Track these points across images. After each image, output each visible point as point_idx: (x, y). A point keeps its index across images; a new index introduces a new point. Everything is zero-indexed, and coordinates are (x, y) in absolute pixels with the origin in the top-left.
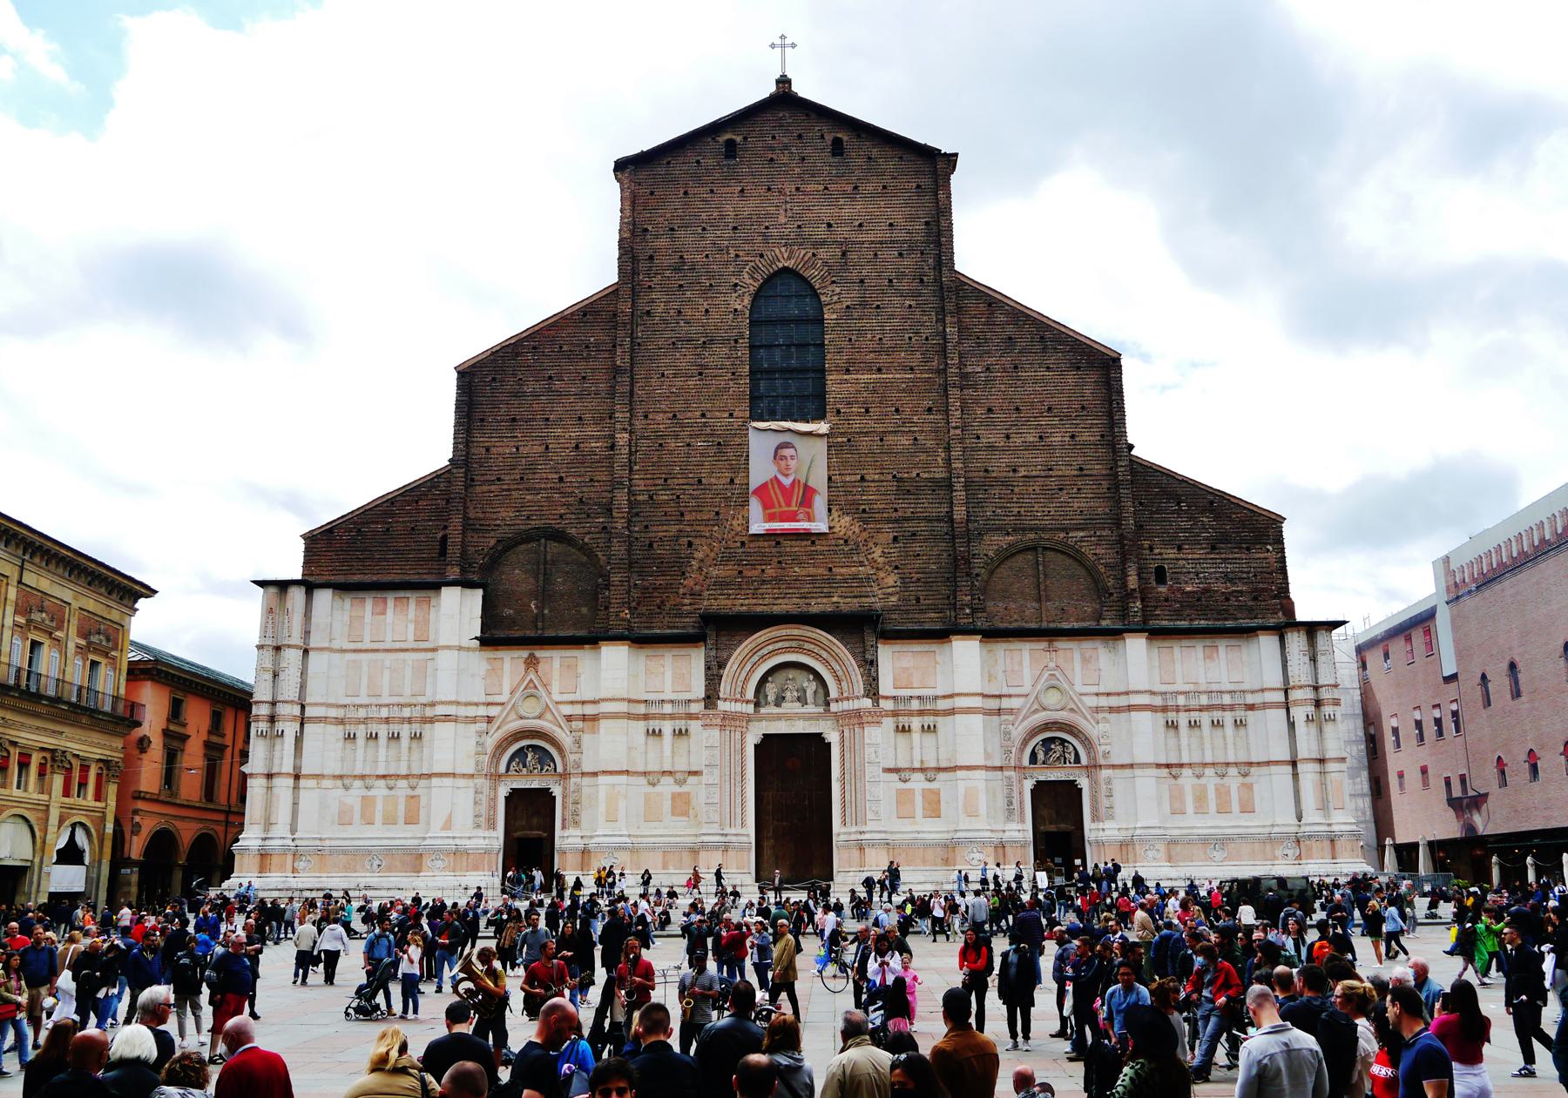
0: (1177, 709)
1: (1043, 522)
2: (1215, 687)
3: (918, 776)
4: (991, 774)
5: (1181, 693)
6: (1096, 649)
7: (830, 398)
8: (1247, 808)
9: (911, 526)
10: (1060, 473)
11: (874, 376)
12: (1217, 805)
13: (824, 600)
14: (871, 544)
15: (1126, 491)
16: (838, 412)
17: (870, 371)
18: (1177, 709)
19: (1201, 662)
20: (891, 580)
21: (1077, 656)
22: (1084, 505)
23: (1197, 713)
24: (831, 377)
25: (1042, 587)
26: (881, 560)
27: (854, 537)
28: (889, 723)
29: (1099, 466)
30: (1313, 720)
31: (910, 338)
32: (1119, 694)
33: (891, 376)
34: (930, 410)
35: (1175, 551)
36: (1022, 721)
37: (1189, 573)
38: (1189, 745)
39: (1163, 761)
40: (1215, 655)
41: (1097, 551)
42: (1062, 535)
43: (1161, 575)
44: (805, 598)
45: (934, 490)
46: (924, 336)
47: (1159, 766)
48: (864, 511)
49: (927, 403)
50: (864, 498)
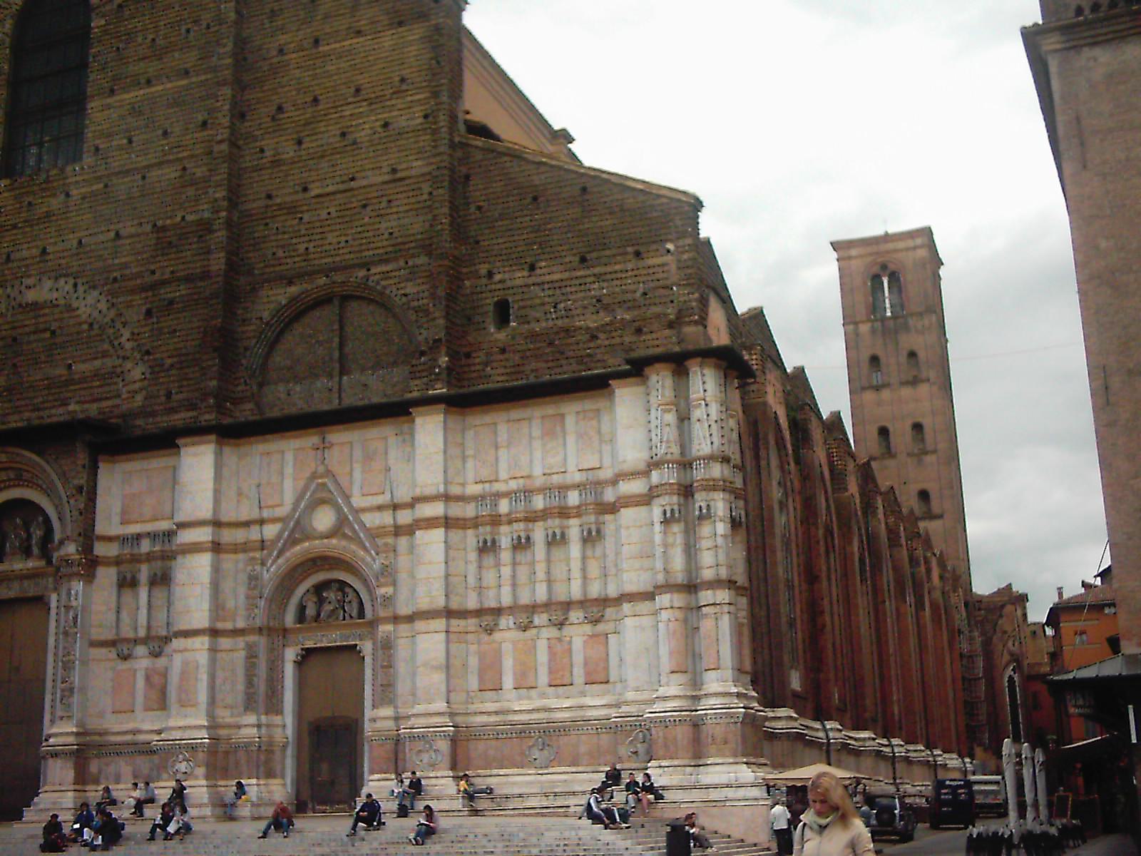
0: (496, 520)
1: (338, 259)
2: (556, 479)
3: (141, 650)
4: (225, 642)
5: (507, 494)
6: (385, 439)
7: (89, 134)
8: (598, 677)
9: (167, 293)
10: (364, 182)
11: (142, 92)
12: (551, 672)
13: (61, 410)
14: (119, 325)
15: (441, 191)
16: (97, 149)
17: (137, 84)
18: (496, 520)
19: (537, 444)
20: (137, 373)
21: (358, 453)
22: (395, 223)
23: (521, 525)
24: (93, 105)
25: (336, 354)
26: (128, 345)
27: (99, 318)
28: (107, 576)
29: (419, 163)
30: (679, 521)
31: (188, 31)
32: (411, 505)
33: (160, 88)
34: (204, 124)
35: (526, 273)
36: (278, 557)
37: (543, 304)
38: (514, 576)
39: (472, 604)
40: (558, 429)
41: (408, 291)
42: (362, 273)
43: (503, 312)
44: (38, 410)
45: (201, 236)
46: (204, 26)
47: (449, 613)
48: (115, 280)
49: (200, 118)
50: (117, 261)
